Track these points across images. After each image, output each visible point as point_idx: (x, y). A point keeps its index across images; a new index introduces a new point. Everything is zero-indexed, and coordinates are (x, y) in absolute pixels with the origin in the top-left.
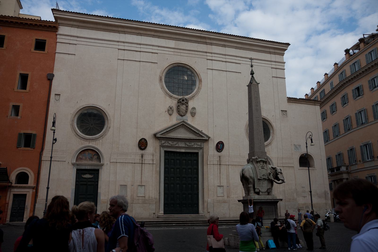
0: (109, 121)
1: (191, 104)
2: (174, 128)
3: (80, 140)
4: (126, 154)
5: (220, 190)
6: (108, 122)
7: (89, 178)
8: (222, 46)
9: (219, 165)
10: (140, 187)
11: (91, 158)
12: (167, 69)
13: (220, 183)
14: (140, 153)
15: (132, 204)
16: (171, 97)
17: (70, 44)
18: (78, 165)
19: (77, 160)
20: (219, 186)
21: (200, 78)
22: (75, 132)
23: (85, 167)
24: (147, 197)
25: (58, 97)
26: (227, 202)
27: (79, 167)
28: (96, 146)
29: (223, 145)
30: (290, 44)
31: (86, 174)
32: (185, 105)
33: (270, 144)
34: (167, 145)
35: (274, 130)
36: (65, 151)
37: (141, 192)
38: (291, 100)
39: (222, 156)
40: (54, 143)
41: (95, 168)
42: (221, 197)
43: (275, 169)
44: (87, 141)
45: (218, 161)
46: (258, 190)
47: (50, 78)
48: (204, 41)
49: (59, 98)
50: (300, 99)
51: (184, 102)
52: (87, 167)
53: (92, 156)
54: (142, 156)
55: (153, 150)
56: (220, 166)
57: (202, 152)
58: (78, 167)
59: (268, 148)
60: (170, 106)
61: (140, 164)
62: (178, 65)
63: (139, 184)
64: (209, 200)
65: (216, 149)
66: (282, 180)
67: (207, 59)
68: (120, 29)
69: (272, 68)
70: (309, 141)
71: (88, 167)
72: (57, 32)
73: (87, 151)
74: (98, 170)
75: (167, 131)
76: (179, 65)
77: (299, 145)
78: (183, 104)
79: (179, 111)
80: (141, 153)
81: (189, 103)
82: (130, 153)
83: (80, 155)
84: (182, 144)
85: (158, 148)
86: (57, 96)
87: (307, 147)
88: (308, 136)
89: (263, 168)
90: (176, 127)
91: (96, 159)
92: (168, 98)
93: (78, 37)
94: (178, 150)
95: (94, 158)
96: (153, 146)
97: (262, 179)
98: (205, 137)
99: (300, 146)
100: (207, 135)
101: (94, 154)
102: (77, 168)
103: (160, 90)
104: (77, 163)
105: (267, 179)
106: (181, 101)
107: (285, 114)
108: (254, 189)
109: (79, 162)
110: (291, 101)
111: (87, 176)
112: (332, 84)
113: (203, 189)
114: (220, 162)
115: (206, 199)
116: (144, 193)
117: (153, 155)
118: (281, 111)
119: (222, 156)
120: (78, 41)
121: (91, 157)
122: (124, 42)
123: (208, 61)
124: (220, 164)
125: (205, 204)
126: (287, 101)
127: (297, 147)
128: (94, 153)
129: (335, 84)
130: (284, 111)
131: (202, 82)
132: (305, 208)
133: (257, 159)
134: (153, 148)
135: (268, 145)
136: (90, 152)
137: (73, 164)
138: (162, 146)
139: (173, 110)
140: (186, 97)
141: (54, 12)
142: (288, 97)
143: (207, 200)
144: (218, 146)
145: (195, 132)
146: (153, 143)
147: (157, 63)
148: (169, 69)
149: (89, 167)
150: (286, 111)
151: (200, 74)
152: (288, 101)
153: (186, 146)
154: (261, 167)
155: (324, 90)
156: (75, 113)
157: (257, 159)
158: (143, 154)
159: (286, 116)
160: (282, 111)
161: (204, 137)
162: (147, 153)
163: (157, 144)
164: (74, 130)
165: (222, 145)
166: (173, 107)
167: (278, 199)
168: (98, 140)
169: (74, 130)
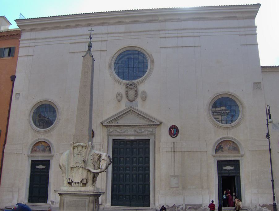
1: (141, 88)
2: (122, 115)
7: (42, 169)
9: (173, 153)
11: (43, 150)
12: (117, 55)
16: (120, 83)
18: (31, 156)
19: (32, 152)
29: (176, 130)
30: (261, 5)
32: (133, 89)
33: (238, 124)
34: (115, 133)
45: (172, 148)
47: (13, 78)
51: (132, 87)
56: (174, 154)
60: (118, 93)
65: (170, 135)
67: (160, 38)
68: (72, 24)
69: (240, 35)
72: (20, 38)
74: (49, 161)
75: (114, 118)
78: (131, 89)
79: (127, 97)
84: (130, 131)
85: (106, 137)
90: (123, 114)
93: (35, 39)
94: (127, 138)
95: (46, 150)
96: (101, 136)
106: (129, 86)
110: (267, 71)
113: (154, 179)
114: (174, 149)
117: (100, 144)
120: (36, 43)
121: (44, 149)
122: (74, 36)
123: (162, 39)
124: (174, 152)
130: (257, 83)
136: (43, 144)
138: (109, 135)
139: (122, 97)
142: (262, 66)
144: (171, 131)
148: (119, 55)
150: (260, 83)
152: (263, 71)
157: (75, 144)
163: (105, 131)
165: (175, 129)
167: (100, 192)
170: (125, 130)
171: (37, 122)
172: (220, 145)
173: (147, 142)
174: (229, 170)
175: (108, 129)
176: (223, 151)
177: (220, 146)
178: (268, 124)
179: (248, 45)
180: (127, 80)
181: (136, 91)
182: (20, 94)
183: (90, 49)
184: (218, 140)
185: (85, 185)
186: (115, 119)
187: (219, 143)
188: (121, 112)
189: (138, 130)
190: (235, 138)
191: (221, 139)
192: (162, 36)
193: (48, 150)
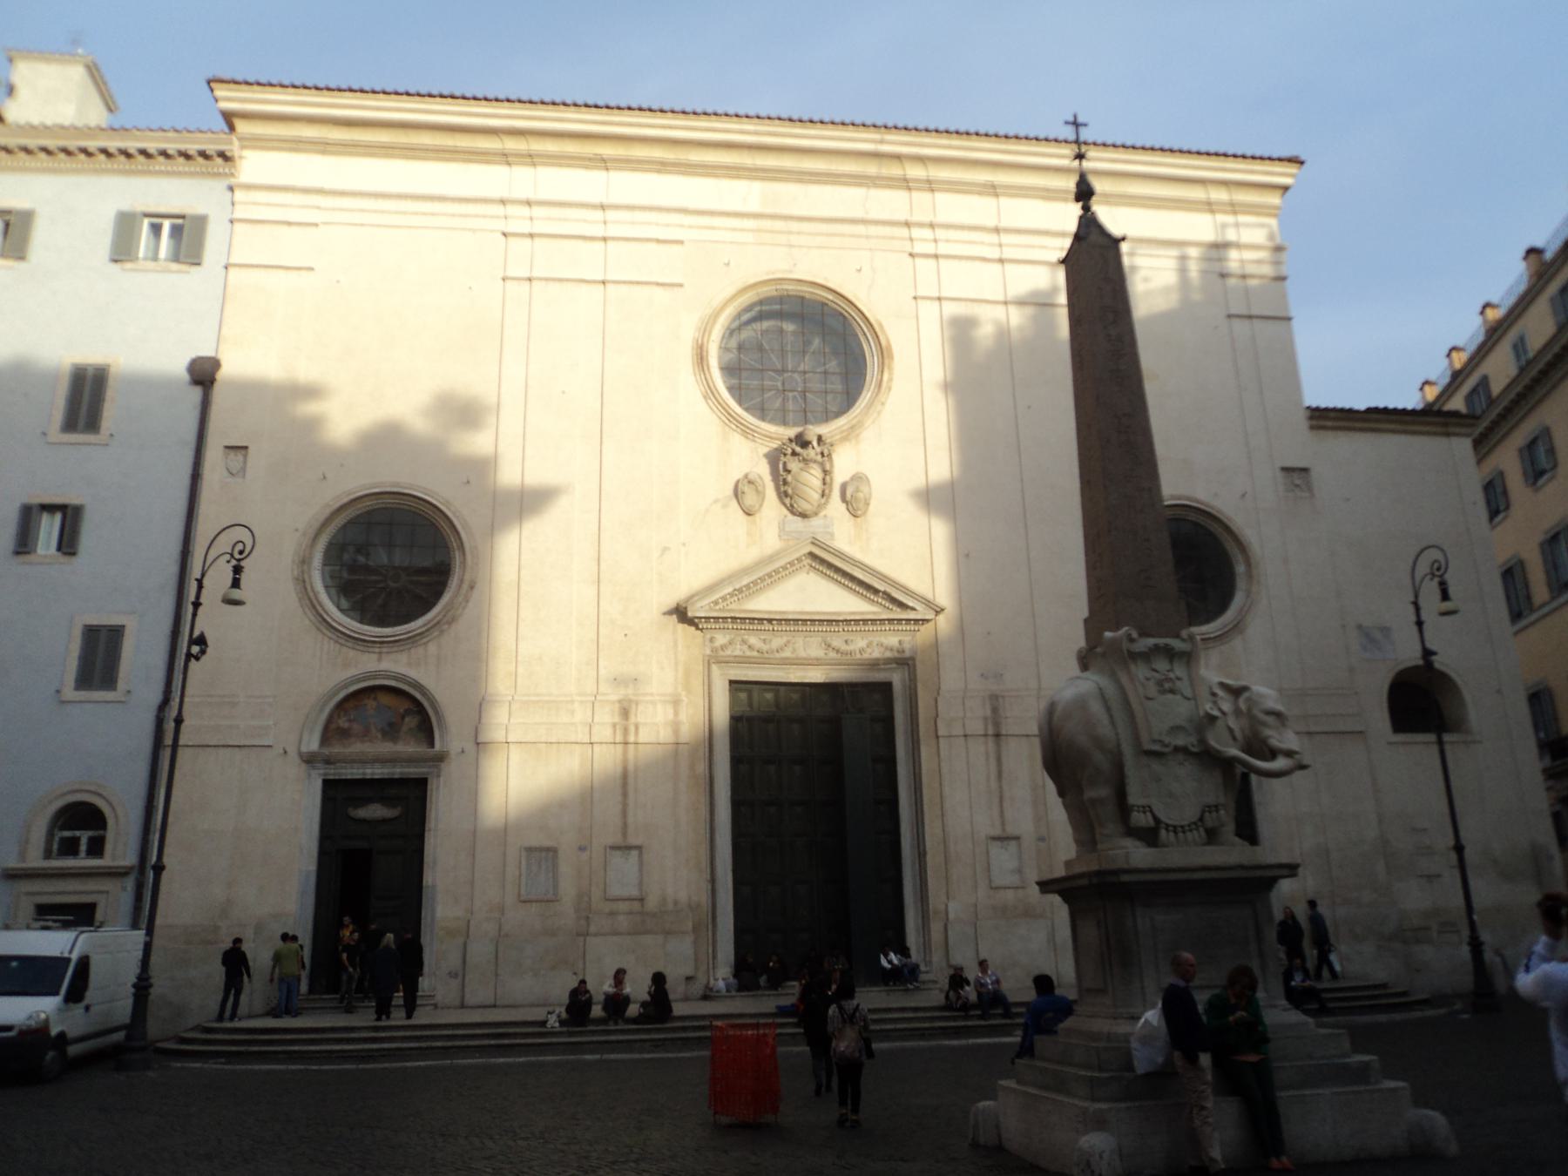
1: (844, 464)
3: (338, 646)
4: (548, 702)
5: (1004, 859)
6: (464, 562)
7: (384, 821)
8: (980, 193)
9: (991, 740)
10: (617, 859)
13: (1003, 824)
14: (614, 698)
15: (582, 939)
16: (747, 432)
17: (289, 224)
18: (328, 761)
19: (325, 740)
23: (361, 771)
24: (652, 903)
25: (240, 457)
27: (332, 771)
28: (413, 674)
32: (815, 466)
33: (1237, 627)
34: (738, 653)
36: (271, 700)
37: (623, 876)
38: (1326, 419)
40: (197, 659)
41: (410, 773)
43: (1246, 695)
44: (371, 650)
46: (1148, 814)
48: (894, 170)
49: (245, 462)
50: (1370, 411)
52: (369, 771)
54: (625, 713)
56: (998, 745)
57: (910, 680)
58: (327, 771)
60: (746, 476)
61: (618, 746)
63: (611, 840)
64: (954, 909)
66: (1289, 754)
68: (511, 144)
70: (1430, 590)
71: (377, 771)
73: (373, 696)
75: (737, 587)
80: (621, 697)
81: (834, 456)
82: (569, 699)
85: (699, 668)
86: (232, 454)
87: (1420, 624)
88: (1423, 568)
89: (1172, 691)
91: (410, 729)
92: (736, 439)
95: (405, 728)
98: (918, 608)
99: (1385, 630)
100: (930, 596)
102: (325, 774)
103: (702, 408)
104: (326, 751)
108: (1124, 809)
109: (337, 749)
110: (1329, 424)
111: (375, 811)
112: (1519, 347)
113: (921, 855)
114: (997, 724)
115: (936, 899)
116: (641, 884)
117: (676, 703)
118: (1285, 469)
119: (1003, 697)
121: (391, 725)
124: (997, 735)
125: (936, 928)
127: (1373, 637)
128: (406, 705)
129: (1535, 343)
135: (1226, 632)
136: (385, 699)
137: (309, 760)
138: (715, 659)
139: (760, 494)
140: (823, 430)
141: (222, 89)
142: (1308, 408)
143: (943, 907)
145: (869, 587)
147: (681, 285)
149: (380, 771)
150: (1305, 470)
152: (1314, 422)
153: (832, 655)
154: (1160, 683)
155: (1484, 381)
156: (317, 525)
158: (630, 701)
161: (913, 609)
162: (647, 694)
164: (311, 602)
169: (311, 602)
170: (785, 639)
175: (708, 636)
180: (777, 424)
181: (825, 472)
182: (250, 451)
185: (1212, 836)
186: (740, 590)
189: (837, 642)
192: (919, 248)
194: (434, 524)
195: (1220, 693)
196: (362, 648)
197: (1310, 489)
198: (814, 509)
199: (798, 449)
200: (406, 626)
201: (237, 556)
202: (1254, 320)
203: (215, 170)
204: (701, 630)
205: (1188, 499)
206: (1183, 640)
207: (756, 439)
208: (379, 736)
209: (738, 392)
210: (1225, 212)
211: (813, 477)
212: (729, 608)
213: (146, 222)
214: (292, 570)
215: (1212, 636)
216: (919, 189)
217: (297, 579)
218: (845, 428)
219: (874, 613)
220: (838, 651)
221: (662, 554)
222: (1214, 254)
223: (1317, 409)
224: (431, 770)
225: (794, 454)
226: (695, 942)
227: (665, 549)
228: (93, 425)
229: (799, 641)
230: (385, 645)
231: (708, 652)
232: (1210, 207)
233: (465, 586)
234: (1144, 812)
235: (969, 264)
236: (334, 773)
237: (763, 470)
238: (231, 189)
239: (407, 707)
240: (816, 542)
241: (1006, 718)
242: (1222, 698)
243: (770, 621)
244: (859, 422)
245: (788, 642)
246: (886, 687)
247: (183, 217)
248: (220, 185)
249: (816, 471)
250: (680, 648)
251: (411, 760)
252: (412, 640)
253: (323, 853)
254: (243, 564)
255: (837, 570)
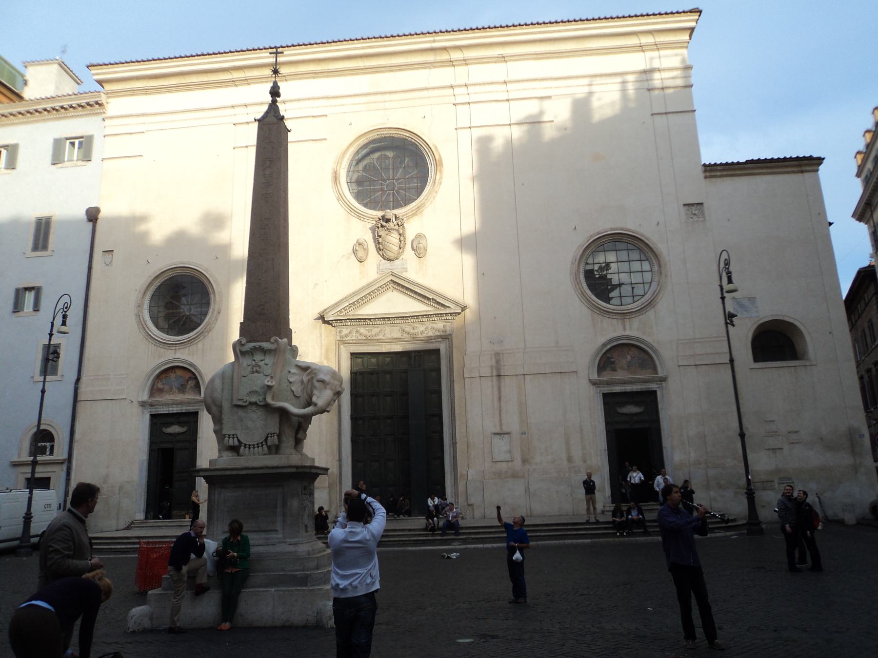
0: (217, 297)
1: (412, 229)
3: (156, 347)
6: (214, 300)
7: (179, 434)
8: (495, 62)
9: (495, 379)
11: (181, 388)
13: (501, 425)
16: (360, 216)
18: (151, 405)
20: (498, 434)
21: (437, 158)
22: (145, 329)
23: (167, 409)
26: (523, 477)
27: (154, 410)
31: (172, 424)
32: (394, 232)
35: (662, 263)
36: (125, 376)
38: (713, 170)
39: (504, 352)
41: (189, 410)
42: (505, 463)
44: (171, 348)
45: (494, 368)
46: (236, 439)
48: (444, 57)
49: (112, 258)
52: (171, 409)
53: (183, 383)
55: (321, 354)
56: (499, 381)
59: (644, 315)
62: (378, 133)
64: (472, 474)
73: (173, 371)
76: (382, 133)
77: (749, 299)
81: (405, 225)
83: (158, 382)
86: (107, 256)
89: (257, 372)
92: (355, 221)
95: (188, 387)
96: (321, 346)
97: (245, 404)
101: (189, 378)
102: (151, 412)
105: (262, 404)
107: (696, 212)
109: (158, 399)
110: (718, 174)
111: (175, 429)
113: (454, 444)
114: (498, 369)
118: (685, 205)
119: (503, 354)
121: (182, 385)
124: (499, 376)
126: (702, 175)
128: (188, 375)
130: (693, 205)
131: (442, 166)
132: (779, 483)
133: (243, 345)
134: (321, 349)
136: (179, 373)
137: (143, 404)
138: (342, 342)
139: (366, 251)
142: (704, 165)
145: (425, 297)
146: (321, 336)
147: (325, 139)
148: (358, 151)
149: (176, 409)
150: (702, 204)
151: (436, 147)
152: (708, 174)
153: (406, 336)
156: (145, 287)
157: (243, 345)
159: (700, 219)
160: (686, 207)
161: (449, 307)
166: (366, 241)
168: (194, 343)
169: (143, 325)
170: (379, 329)
171: (161, 320)
172: (608, 355)
173: (433, 357)
174: (631, 415)
176: (616, 370)
177: (609, 358)
178: (723, 298)
179: (669, 113)
180: (379, 210)
183: (276, 101)
184: (604, 345)
185: (275, 449)
187: (604, 350)
188: (369, 286)
189: (408, 329)
190: (645, 338)
191: (610, 341)
192: (459, 100)
193: (191, 387)
194: (201, 281)
195: (293, 370)
196: (167, 347)
197: (703, 215)
198: (396, 256)
199: (384, 224)
200: (187, 335)
201: (65, 310)
202: (669, 115)
203: (96, 112)
204: (334, 326)
205: (622, 229)
206: (273, 343)
207: (365, 220)
208: (177, 391)
209: (359, 196)
210: (652, 50)
211: (393, 239)
212: (348, 314)
213: (68, 142)
214: (134, 311)
215: (634, 310)
216: (460, 65)
217: (136, 315)
218: (414, 208)
219: (426, 311)
220: (408, 334)
221: (315, 286)
222: (644, 77)
223: (710, 165)
224: (200, 407)
225: (382, 226)
226: (329, 493)
227: (316, 284)
228: (45, 247)
229: (387, 329)
230: (178, 345)
231: (338, 338)
232: (641, 48)
233: (216, 312)
234: (233, 438)
235: (489, 104)
236: (155, 411)
237: (369, 238)
238: (104, 120)
239: (189, 376)
240: (393, 274)
241: (504, 366)
242: (294, 374)
243: (369, 319)
244: (422, 204)
245: (381, 330)
246: (437, 352)
247: (82, 137)
248: (98, 119)
249: (395, 235)
250: (323, 337)
251: (189, 403)
252: (190, 342)
253: (151, 451)
254: (67, 313)
255: (407, 289)
